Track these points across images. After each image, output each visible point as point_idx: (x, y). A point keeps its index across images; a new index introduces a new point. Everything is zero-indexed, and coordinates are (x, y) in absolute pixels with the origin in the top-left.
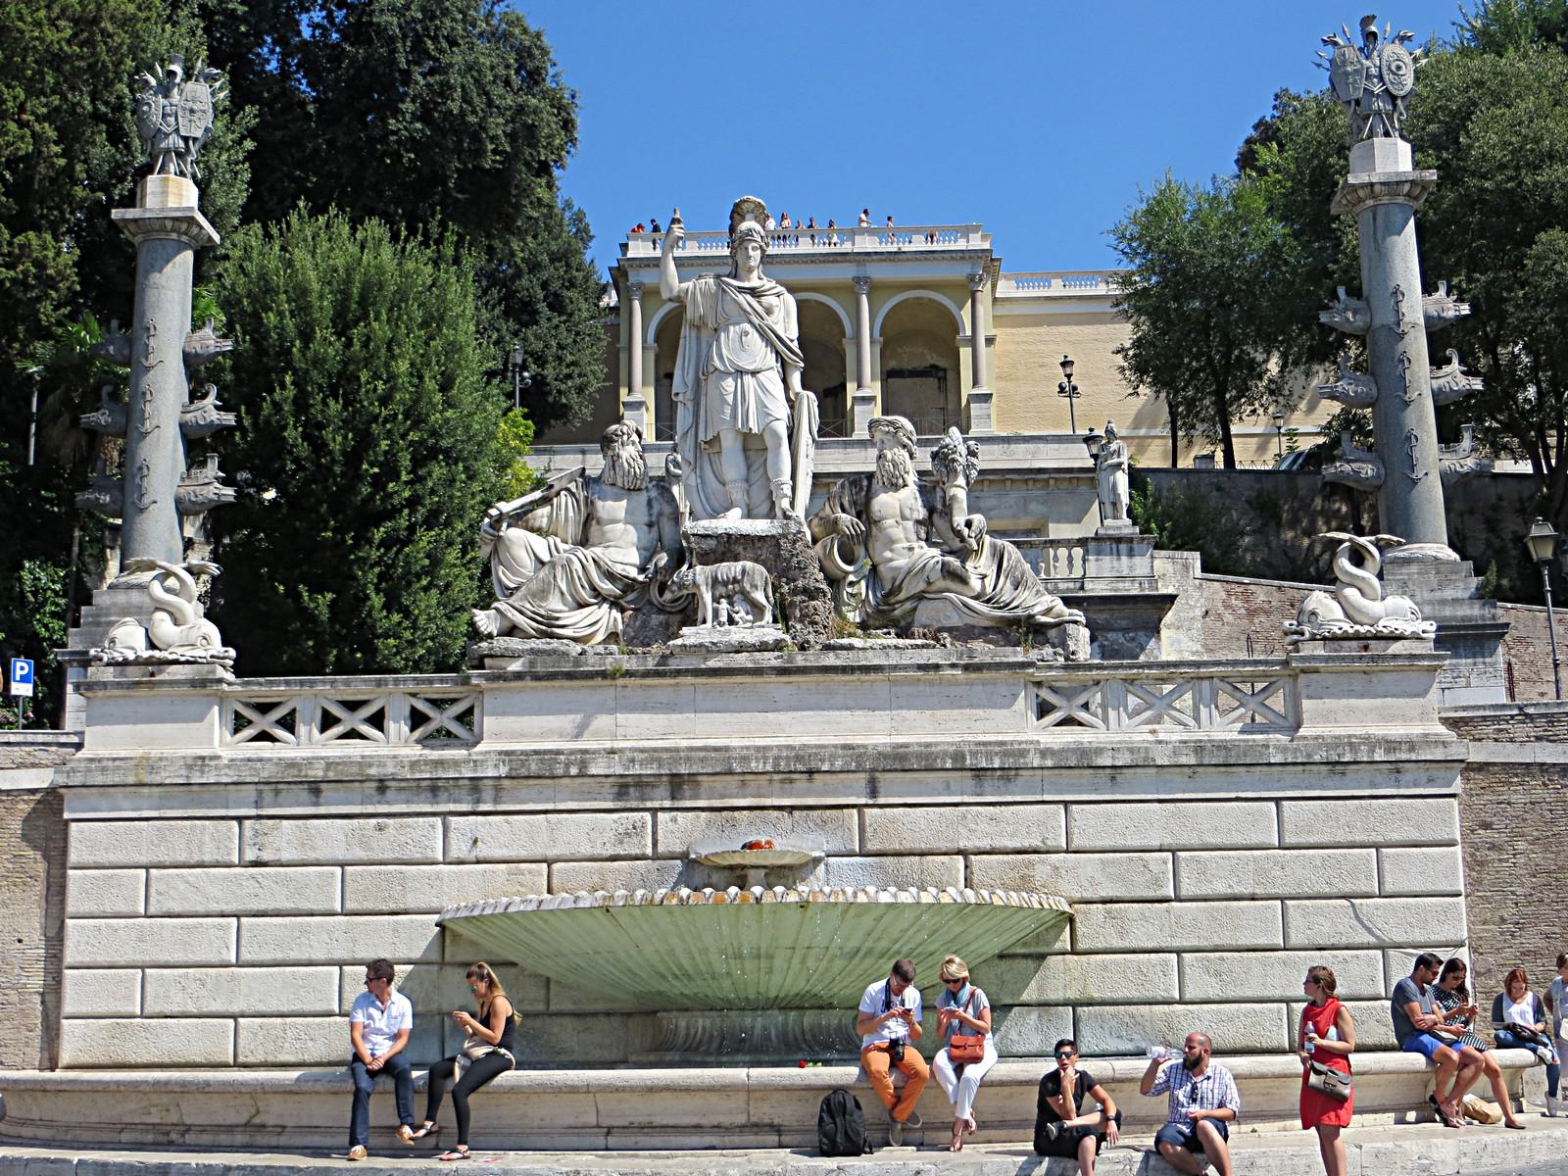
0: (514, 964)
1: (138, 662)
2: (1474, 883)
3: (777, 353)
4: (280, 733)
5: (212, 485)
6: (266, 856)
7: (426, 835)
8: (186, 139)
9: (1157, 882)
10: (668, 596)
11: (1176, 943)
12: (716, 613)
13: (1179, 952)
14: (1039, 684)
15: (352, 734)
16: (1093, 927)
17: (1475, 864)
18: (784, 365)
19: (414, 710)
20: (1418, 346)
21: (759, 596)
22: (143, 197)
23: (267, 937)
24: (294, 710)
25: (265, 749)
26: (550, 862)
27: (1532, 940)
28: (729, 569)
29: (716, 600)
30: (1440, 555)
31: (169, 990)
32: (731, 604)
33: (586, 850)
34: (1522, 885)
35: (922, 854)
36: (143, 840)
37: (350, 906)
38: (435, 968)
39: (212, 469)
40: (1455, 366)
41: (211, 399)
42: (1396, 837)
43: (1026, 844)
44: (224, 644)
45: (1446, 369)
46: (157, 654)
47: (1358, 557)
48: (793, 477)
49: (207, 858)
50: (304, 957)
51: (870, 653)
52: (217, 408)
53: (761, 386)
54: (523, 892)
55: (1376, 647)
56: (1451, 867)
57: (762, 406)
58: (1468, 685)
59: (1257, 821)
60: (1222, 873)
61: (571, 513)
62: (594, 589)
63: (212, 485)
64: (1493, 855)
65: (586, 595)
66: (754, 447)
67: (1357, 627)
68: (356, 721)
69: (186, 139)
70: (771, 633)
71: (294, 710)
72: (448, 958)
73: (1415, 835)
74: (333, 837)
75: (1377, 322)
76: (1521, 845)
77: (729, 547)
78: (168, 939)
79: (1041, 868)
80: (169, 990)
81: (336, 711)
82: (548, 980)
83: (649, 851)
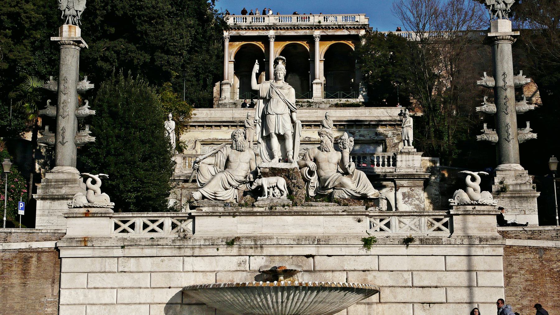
0: (205, 304)
1: (85, 207)
2: (507, 284)
3: (289, 108)
4: (130, 230)
5: (87, 137)
6: (126, 270)
7: (177, 264)
8: (77, 11)
9: (406, 281)
11: (412, 301)
12: (268, 193)
13: (413, 303)
15: (153, 231)
16: (386, 294)
17: (508, 277)
18: (291, 112)
19: (173, 223)
20: (510, 94)
21: (283, 189)
22: (62, 32)
24: (134, 223)
25: (124, 235)
26: (216, 273)
27: (525, 302)
28: (273, 180)
29: (268, 188)
30: (516, 168)
32: (274, 190)
34: (522, 285)
35: (333, 271)
36: (87, 265)
37: (152, 286)
38: (179, 305)
39: (87, 130)
41: (87, 105)
42: (482, 269)
43: (365, 268)
44: (111, 201)
45: (521, 103)
46: (90, 204)
47: (473, 179)
48: (294, 149)
49: (107, 270)
50: (138, 302)
51: (317, 208)
52: (89, 108)
53: (284, 119)
55: (478, 208)
56: (499, 279)
57: (284, 126)
58: (525, 214)
59: (439, 263)
61: (222, 159)
62: (229, 183)
63: (87, 137)
64: (513, 275)
65: (228, 186)
67: (472, 202)
68: (154, 226)
69: (77, 11)
71: (134, 223)
72: (184, 302)
73: (488, 269)
76: (523, 272)
79: (370, 277)
81: (148, 223)
82: (216, 309)
83: (248, 269)
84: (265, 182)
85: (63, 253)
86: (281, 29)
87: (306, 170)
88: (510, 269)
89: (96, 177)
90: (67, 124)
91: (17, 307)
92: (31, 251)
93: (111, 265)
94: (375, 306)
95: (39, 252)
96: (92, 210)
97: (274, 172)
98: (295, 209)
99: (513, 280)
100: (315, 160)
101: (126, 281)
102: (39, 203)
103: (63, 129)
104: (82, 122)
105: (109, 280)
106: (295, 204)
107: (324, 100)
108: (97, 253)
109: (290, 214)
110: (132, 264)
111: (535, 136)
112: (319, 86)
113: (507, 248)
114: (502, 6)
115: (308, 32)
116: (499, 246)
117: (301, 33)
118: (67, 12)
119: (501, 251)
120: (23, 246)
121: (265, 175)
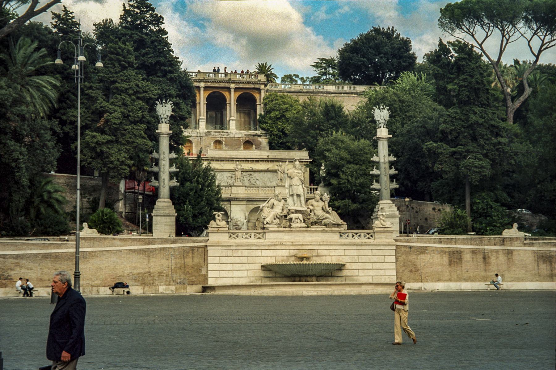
2: (396, 261)
5: (175, 183)
7: (258, 253)
10: (287, 218)
14: (340, 233)
16: (348, 266)
17: (396, 258)
20: (387, 166)
23: (237, 267)
31: (223, 274)
33: (280, 255)
39: (175, 180)
40: (393, 169)
54: (272, 261)
55: (386, 229)
56: (393, 259)
59: (369, 252)
60: (364, 259)
63: (175, 183)
66: (298, 196)
70: (304, 225)
74: (246, 253)
75: (381, 161)
77: (297, 211)
78: (223, 267)
79: (341, 258)
80: (223, 274)
84: (293, 216)
85: (209, 248)
86: (208, 82)
87: (309, 210)
88: (398, 255)
89: (219, 213)
90: (165, 176)
91: (190, 272)
92: (195, 247)
93: (229, 253)
94: (343, 271)
95: (198, 247)
96: (220, 229)
97: (297, 211)
98: (309, 229)
99: (400, 259)
100: (312, 205)
101: (237, 260)
102: (154, 218)
103: (164, 179)
104: (172, 176)
105: (230, 260)
106: (308, 227)
107: (237, 131)
108: (224, 248)
109: (307, 231)
110: (239, 253)
111: (398, 186)
112: (234, 122)
113: (397, 246)
114: (383, 121)
115: (227, 85)
116: (393, 245)
117: (222, 85)
118: (162, 116)
119: (395, 248)
120: (192, 245)
121: (293, 213)
